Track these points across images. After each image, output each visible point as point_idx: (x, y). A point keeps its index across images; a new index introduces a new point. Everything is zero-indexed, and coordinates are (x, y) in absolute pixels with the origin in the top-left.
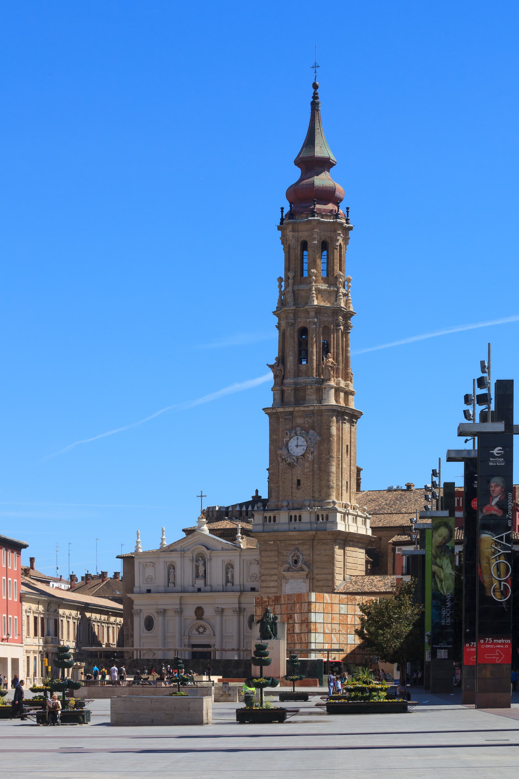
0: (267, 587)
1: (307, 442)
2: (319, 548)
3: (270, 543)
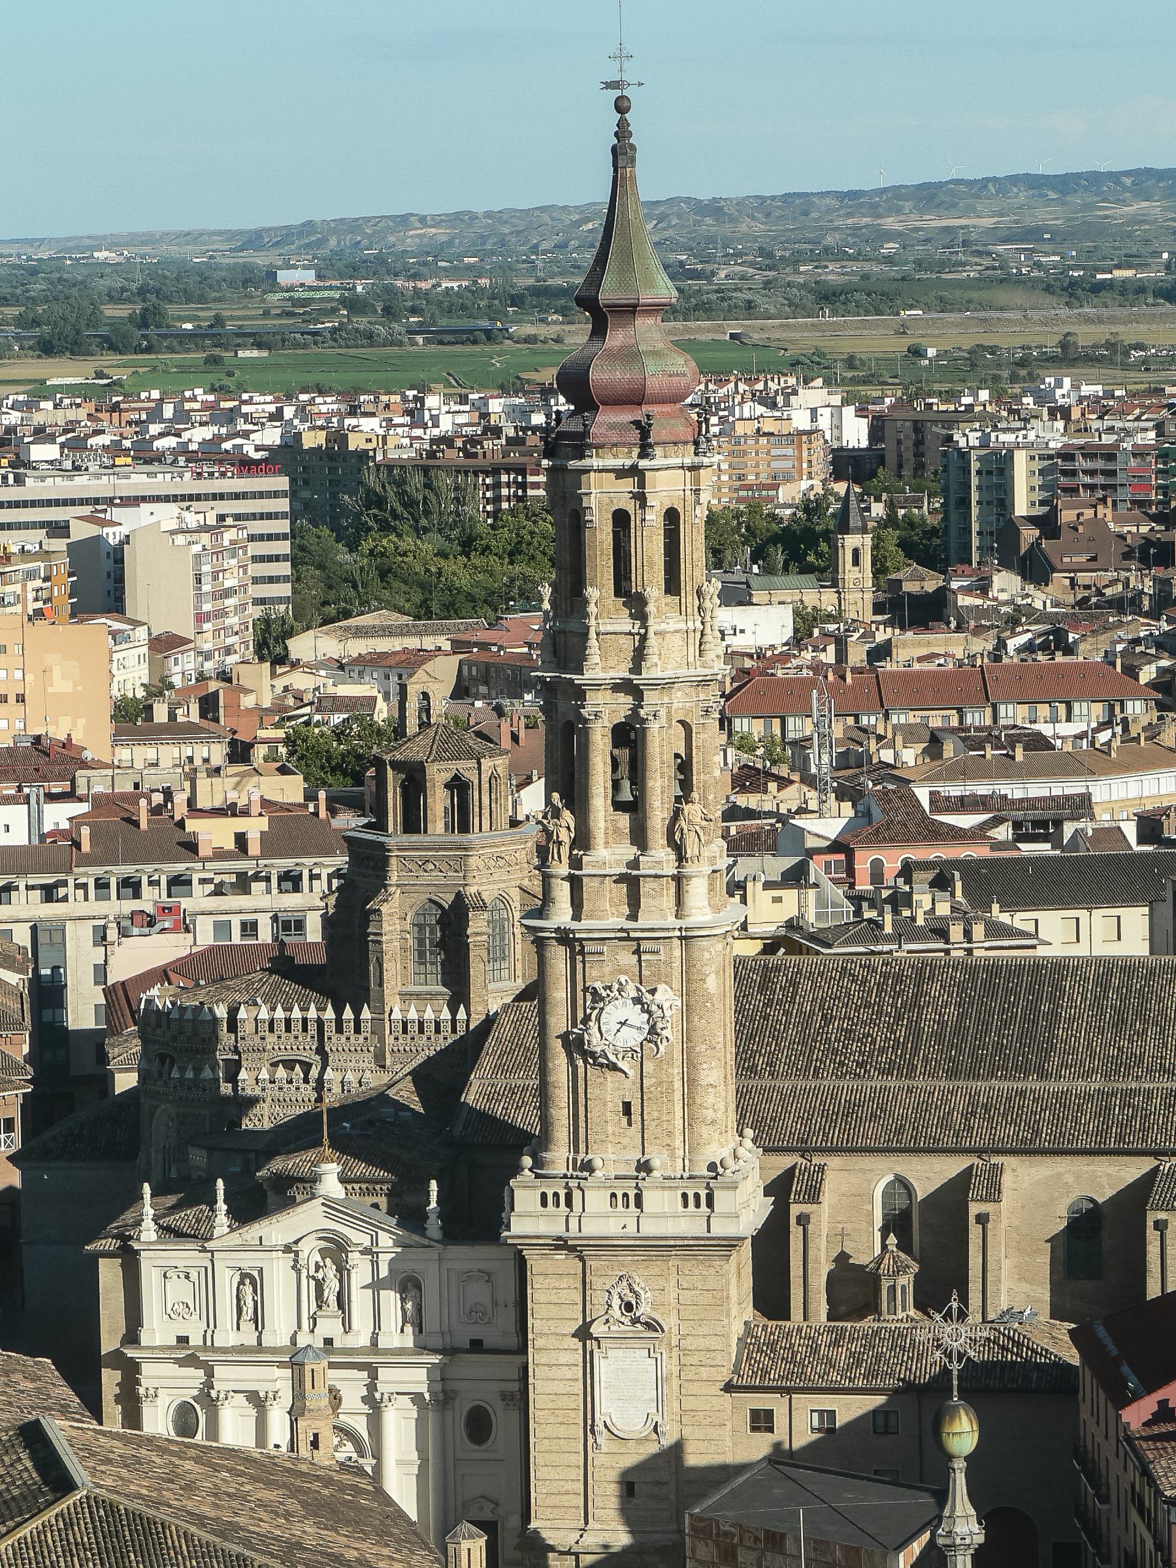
1: (650, 1016)
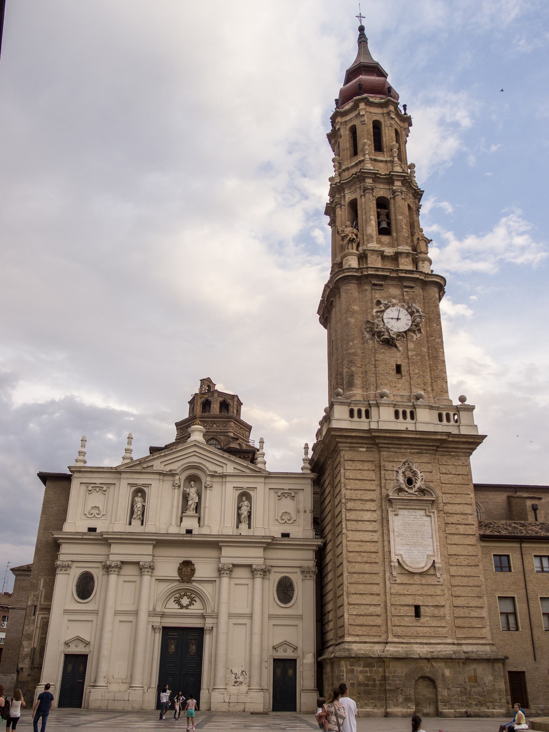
1: (411, 316)
3: (361, 449)
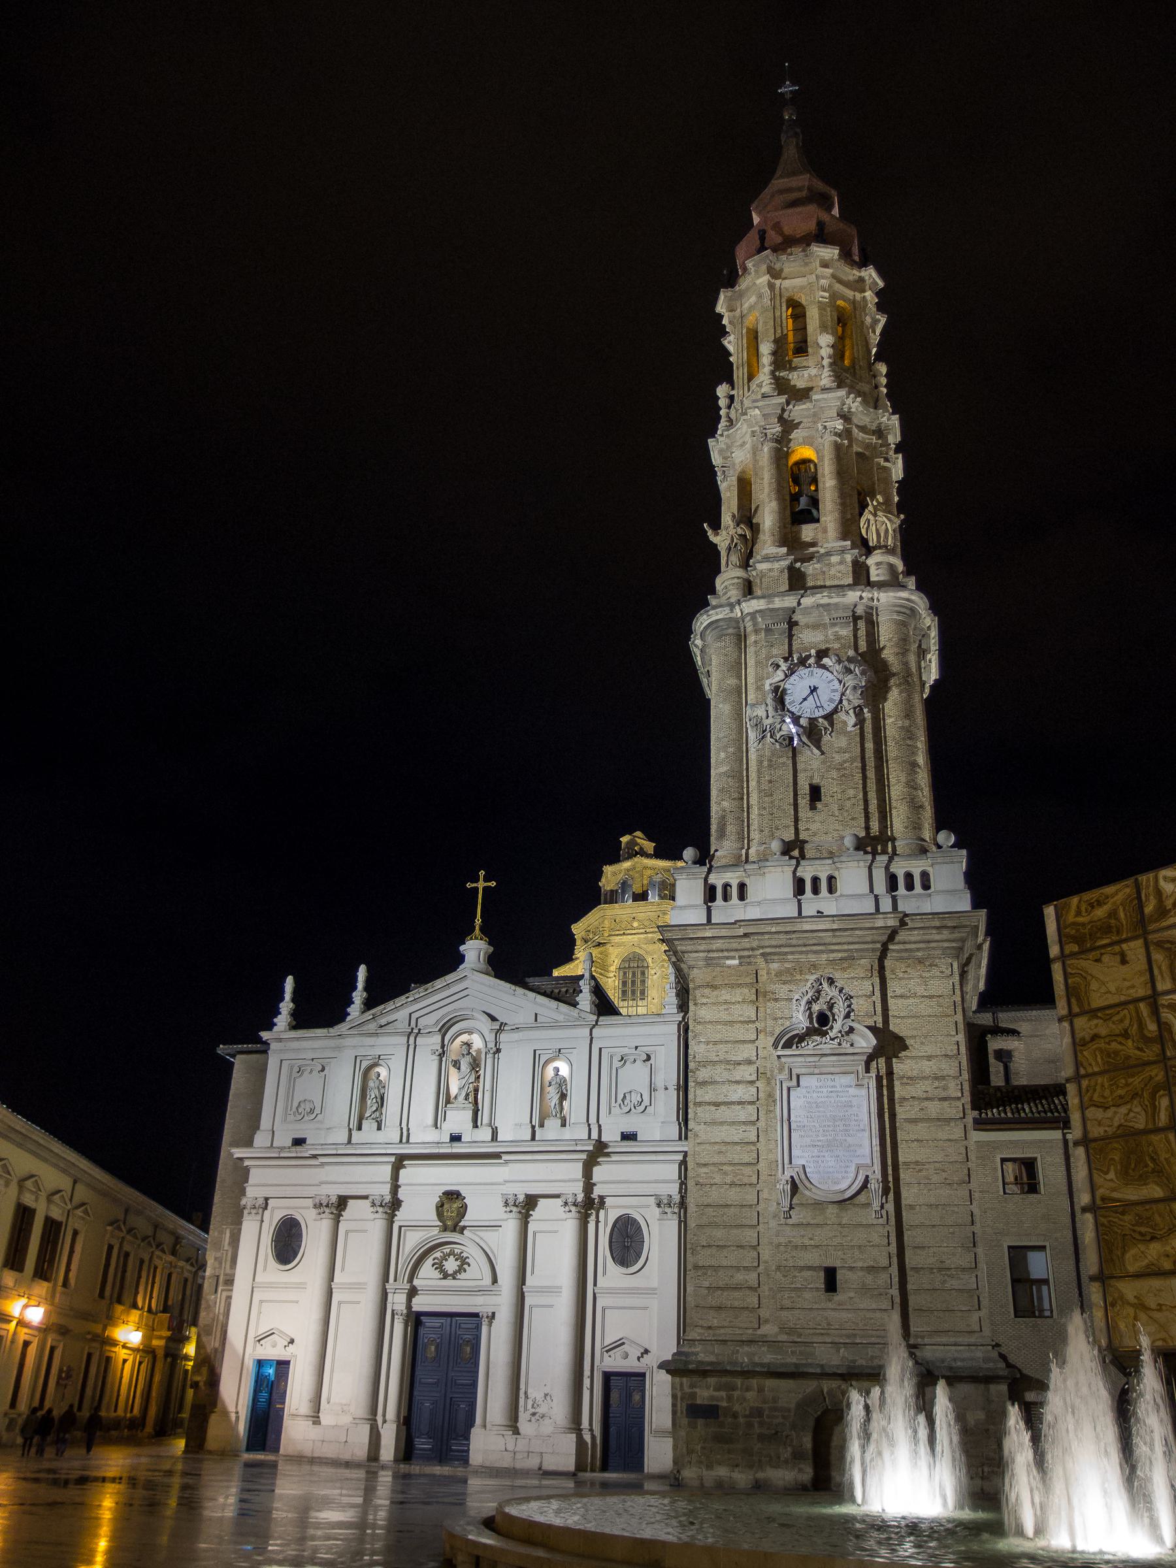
0: (717, 1105)
2: (901, 975)
3: (729, 962)
